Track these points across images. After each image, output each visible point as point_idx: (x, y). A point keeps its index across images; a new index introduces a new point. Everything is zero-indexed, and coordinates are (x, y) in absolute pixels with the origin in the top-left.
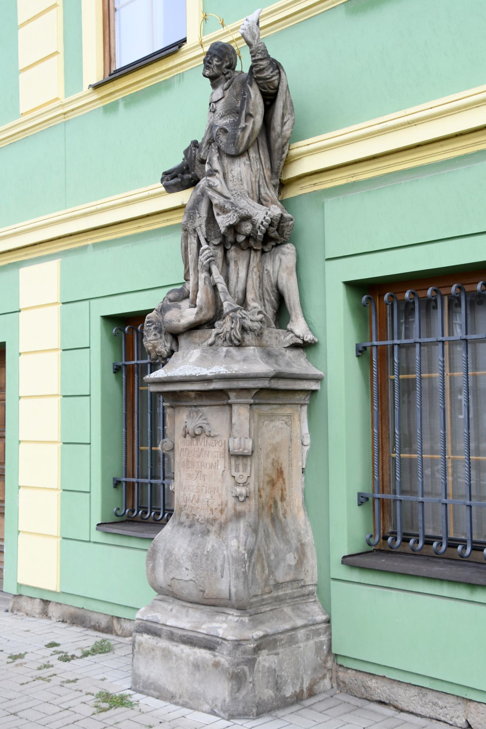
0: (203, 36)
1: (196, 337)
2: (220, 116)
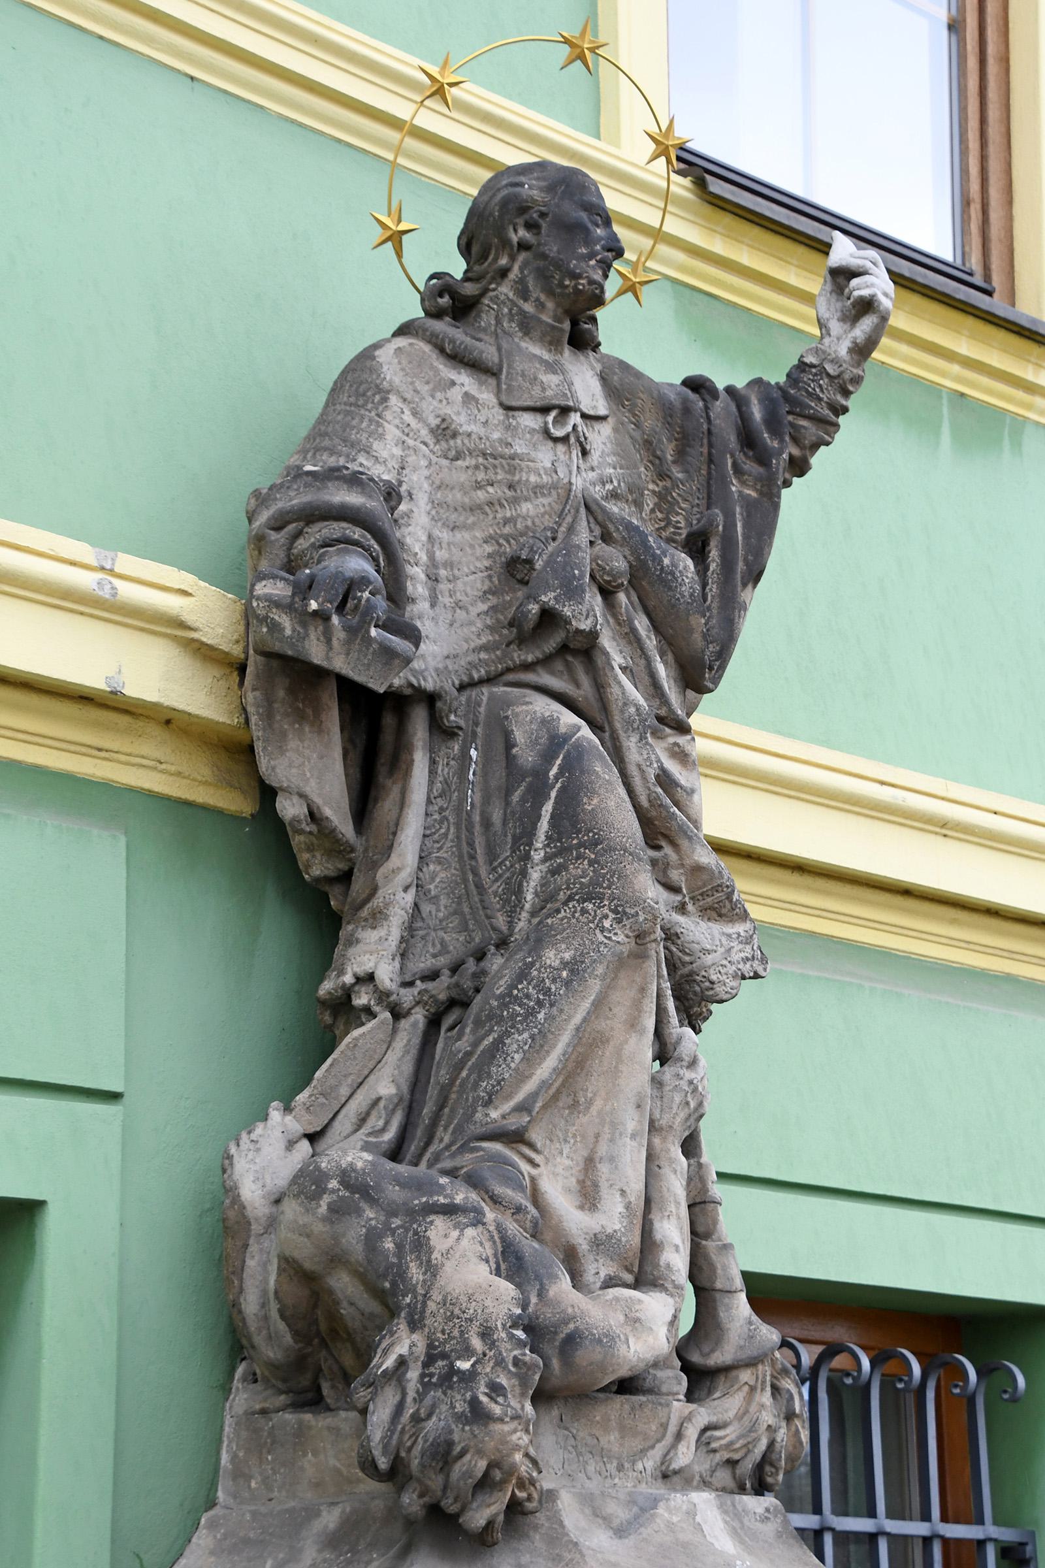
0: (618, 146)
1: (605, 1426)
2: (609, 487)
